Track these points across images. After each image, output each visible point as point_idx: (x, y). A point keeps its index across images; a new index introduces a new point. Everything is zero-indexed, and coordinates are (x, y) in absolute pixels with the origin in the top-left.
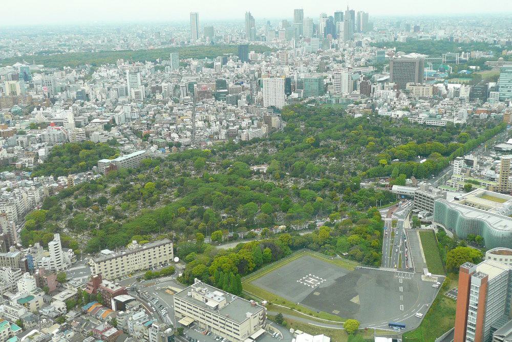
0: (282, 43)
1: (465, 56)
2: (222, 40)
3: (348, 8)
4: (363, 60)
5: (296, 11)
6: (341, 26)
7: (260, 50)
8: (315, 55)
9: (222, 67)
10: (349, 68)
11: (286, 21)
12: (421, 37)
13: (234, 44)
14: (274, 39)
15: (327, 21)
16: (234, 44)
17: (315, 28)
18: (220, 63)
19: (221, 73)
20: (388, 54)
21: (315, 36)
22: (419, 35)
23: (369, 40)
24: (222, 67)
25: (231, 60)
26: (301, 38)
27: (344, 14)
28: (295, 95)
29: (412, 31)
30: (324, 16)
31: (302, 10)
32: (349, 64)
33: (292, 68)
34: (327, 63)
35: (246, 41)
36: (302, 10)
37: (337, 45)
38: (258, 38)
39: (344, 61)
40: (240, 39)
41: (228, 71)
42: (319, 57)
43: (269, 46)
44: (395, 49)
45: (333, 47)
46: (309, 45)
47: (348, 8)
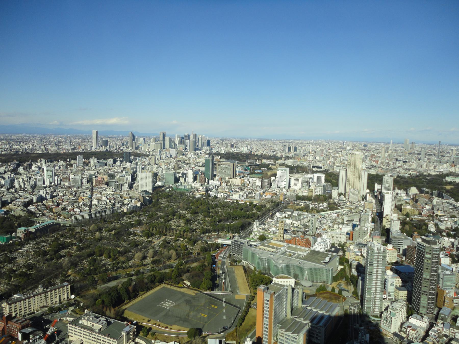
1: (258, 162)
2: (114, 149)
4: (201, 163)
7: (137, 155)
12: (234, 151)
21: (173, 148)
28: (159, 183)
38: (137, 148)
40: (125, 148)
41: (116, 168)
42: (174, 161)
44: (220, 157)
45: (183, 155)
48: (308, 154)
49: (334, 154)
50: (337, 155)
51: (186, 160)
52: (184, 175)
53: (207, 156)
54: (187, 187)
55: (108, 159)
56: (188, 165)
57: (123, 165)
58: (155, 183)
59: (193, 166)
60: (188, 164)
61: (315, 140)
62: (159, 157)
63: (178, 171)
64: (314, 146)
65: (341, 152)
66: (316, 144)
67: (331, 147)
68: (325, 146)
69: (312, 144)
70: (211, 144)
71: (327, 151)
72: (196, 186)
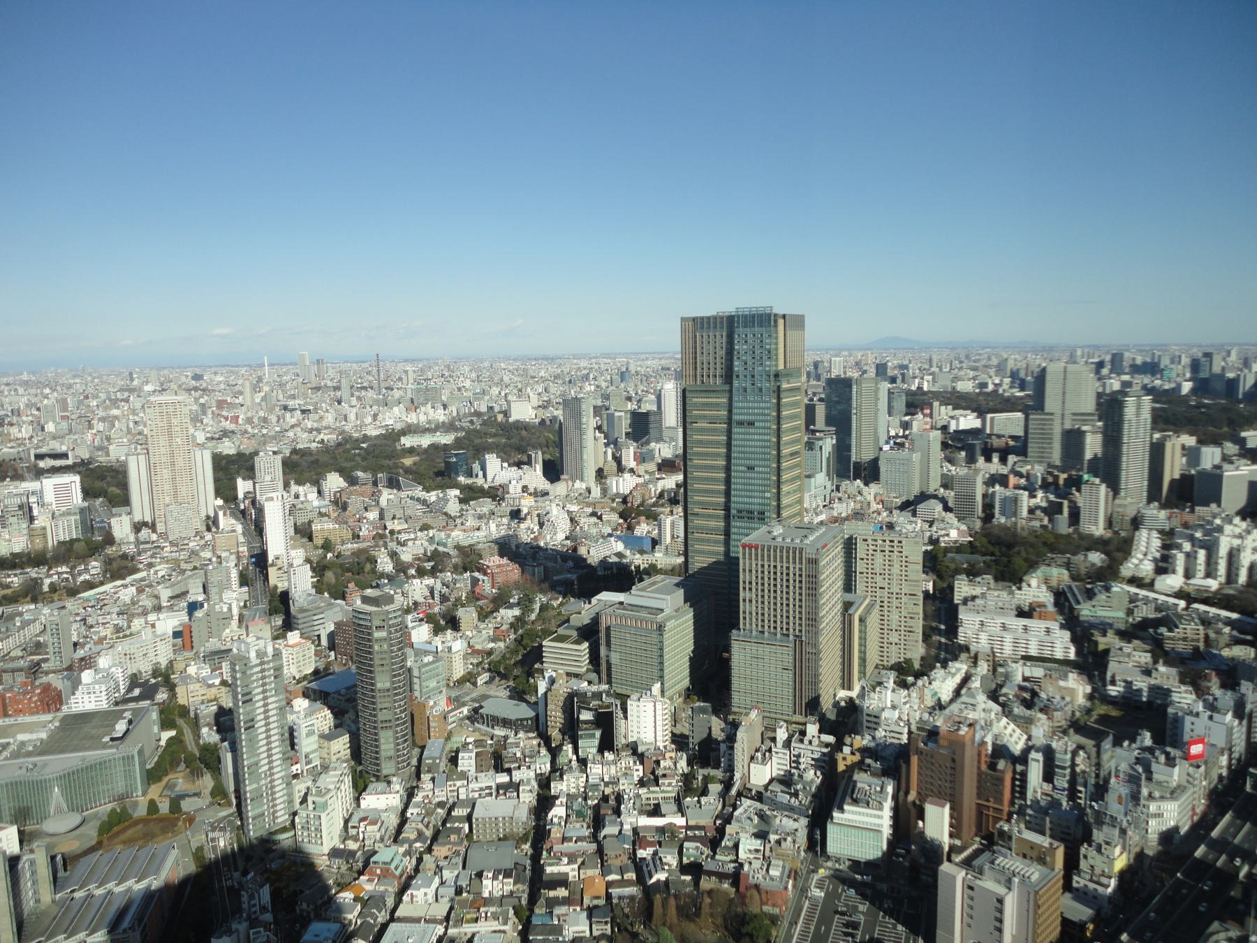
48: (15, 419)
49: (106, 408)
50: (115, 412)
61: (34, 373)
64: (33, 391)
65: (127, 400)
66: (40, 384)
67: (90, 390)
68: (70, 387)
69: (26, 384)
71: (80, 402)
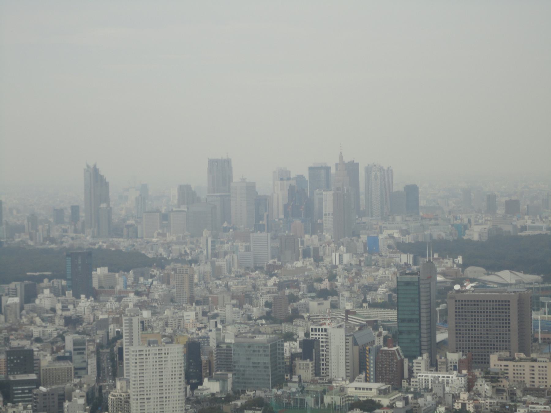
0: (176, 243)
2: (24, 237)
3: (341, 157)
4: (382, 289)
5: (213, 163)
6: (327, 201)
7: (121, 262)
8: (263, 276)
9: (22, 309)
10: (348, 312)
11: (188, 187)
12: (524, 228)
13: (53, 246)
14: (159, 234)
15: (291, 189)
16: (53, 246)
17: (260, 203)
18: (16, 300)
19: (21, 325)
20: (444, 274)
22: (519, 224)
23: (396, 235)
24: (22, 309)
25: (47, 292)
26: (226, 230)
27: (333, 171)
28: (210, 387)
29: (501, 211)
30: (283, 176)
31: (228, 161)
32: (348, 300)
33: (204, 314)
34: (293, 299)
35: (86, 240)
36: (228, 161)
37: (316, 250)
38: (117, 231)
39: (333, 292)
41: (38, 320)
43: (143, 252)
44: (460, 260)
45: (306, 254)
46: (248, 249)
47: (341, 157)
51: (320, 280)
52: (310, 348)
53: (406, 259)
54: (327, 399)
55: (9, 282)
56: (327, 304)
57: (65, 308)
58: (194, 387)
59: (349, 306)
60: (324, 294)
62: (208, 268)
63: (286, 328)
70: (423, 203)
72: (363, 395)
